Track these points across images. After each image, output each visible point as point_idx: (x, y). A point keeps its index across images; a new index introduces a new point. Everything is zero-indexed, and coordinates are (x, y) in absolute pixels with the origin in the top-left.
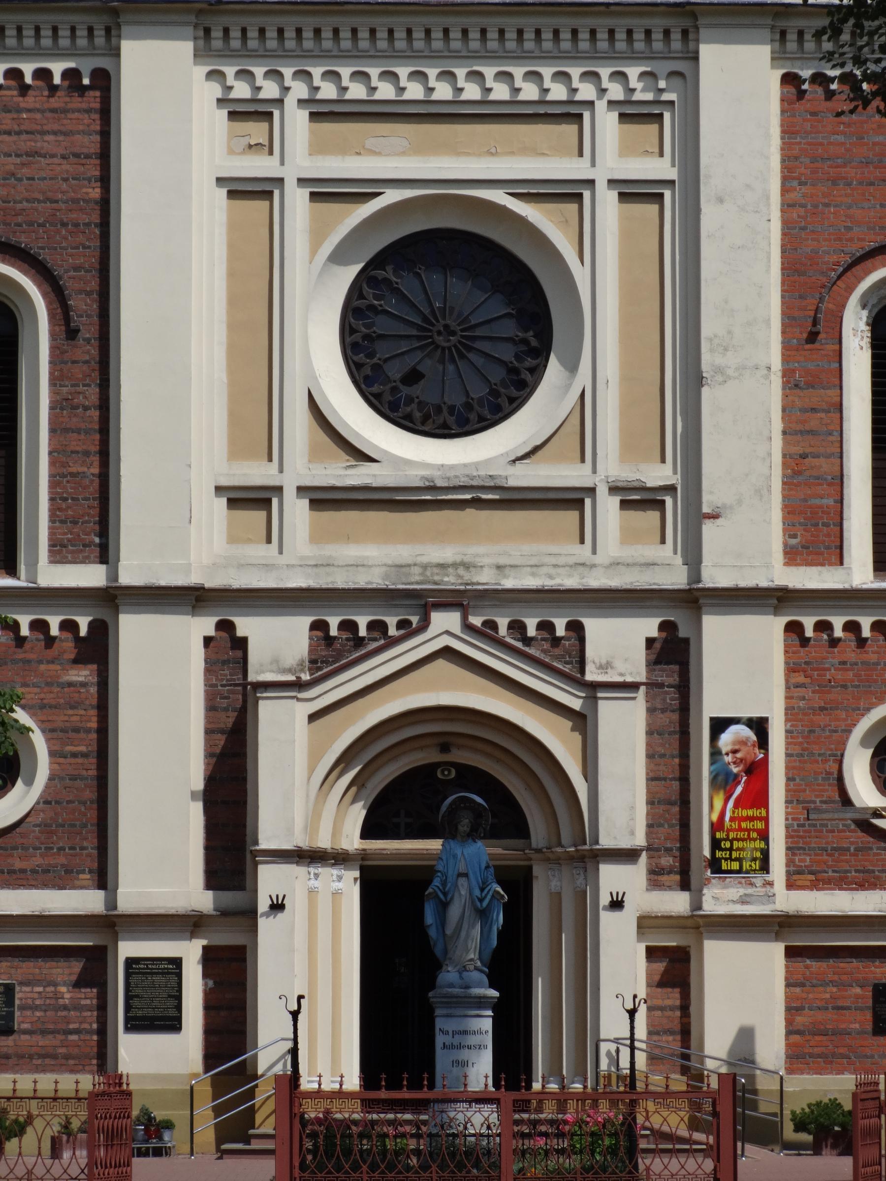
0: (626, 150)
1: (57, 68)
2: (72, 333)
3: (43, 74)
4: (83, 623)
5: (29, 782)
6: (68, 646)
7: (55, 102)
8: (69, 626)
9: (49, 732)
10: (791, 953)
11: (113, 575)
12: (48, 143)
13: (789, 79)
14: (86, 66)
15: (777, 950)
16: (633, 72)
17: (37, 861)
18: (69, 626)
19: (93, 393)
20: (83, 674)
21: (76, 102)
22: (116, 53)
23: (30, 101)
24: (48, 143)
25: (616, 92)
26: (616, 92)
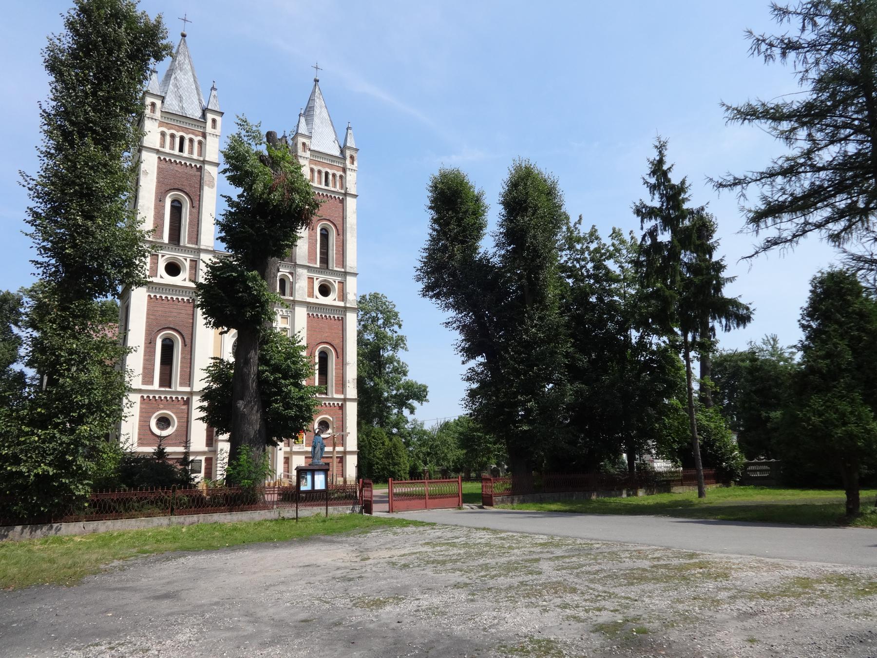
0: (282, 323)
1: (186, 299)
2: (185, 345)
3: (183, 299)
4: (185, 398)
5: (173, 427)
6: (182, 402)
7: (185, 304)
8: (182, 398)
9: (178, 417)
10: (306, 458)
11: (192, 389)
12: (183, 311)
13: (308, 314)
14: (340, 317)
15: (304, 457)
16: (284, 310)
17: (174, 442)
18: (182, 398)
19: (189, 357)
20: (185, 407)
21: (188, 305)
22: (346, 315)
23: (180, 304)
24: (183, 311)
25: (281, 313)
26: (281, 313)
